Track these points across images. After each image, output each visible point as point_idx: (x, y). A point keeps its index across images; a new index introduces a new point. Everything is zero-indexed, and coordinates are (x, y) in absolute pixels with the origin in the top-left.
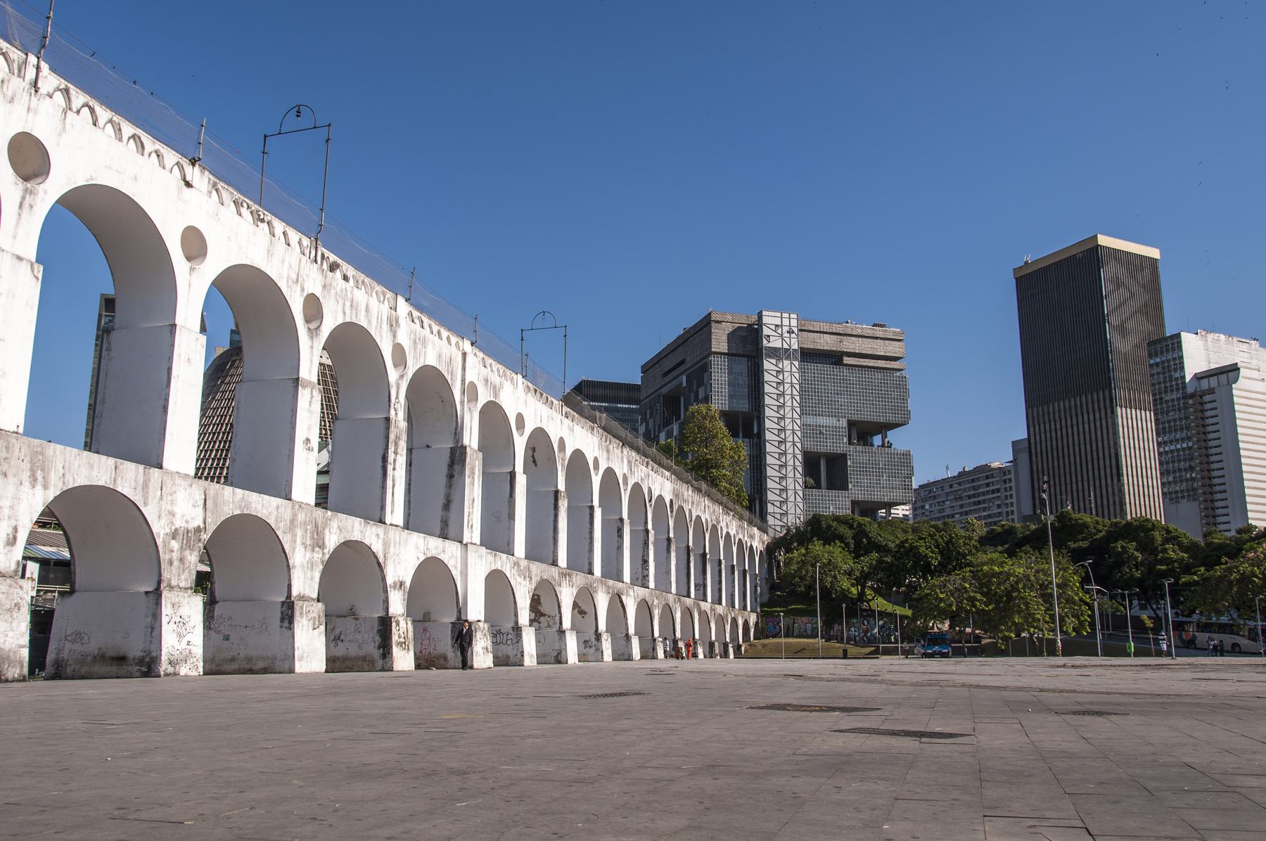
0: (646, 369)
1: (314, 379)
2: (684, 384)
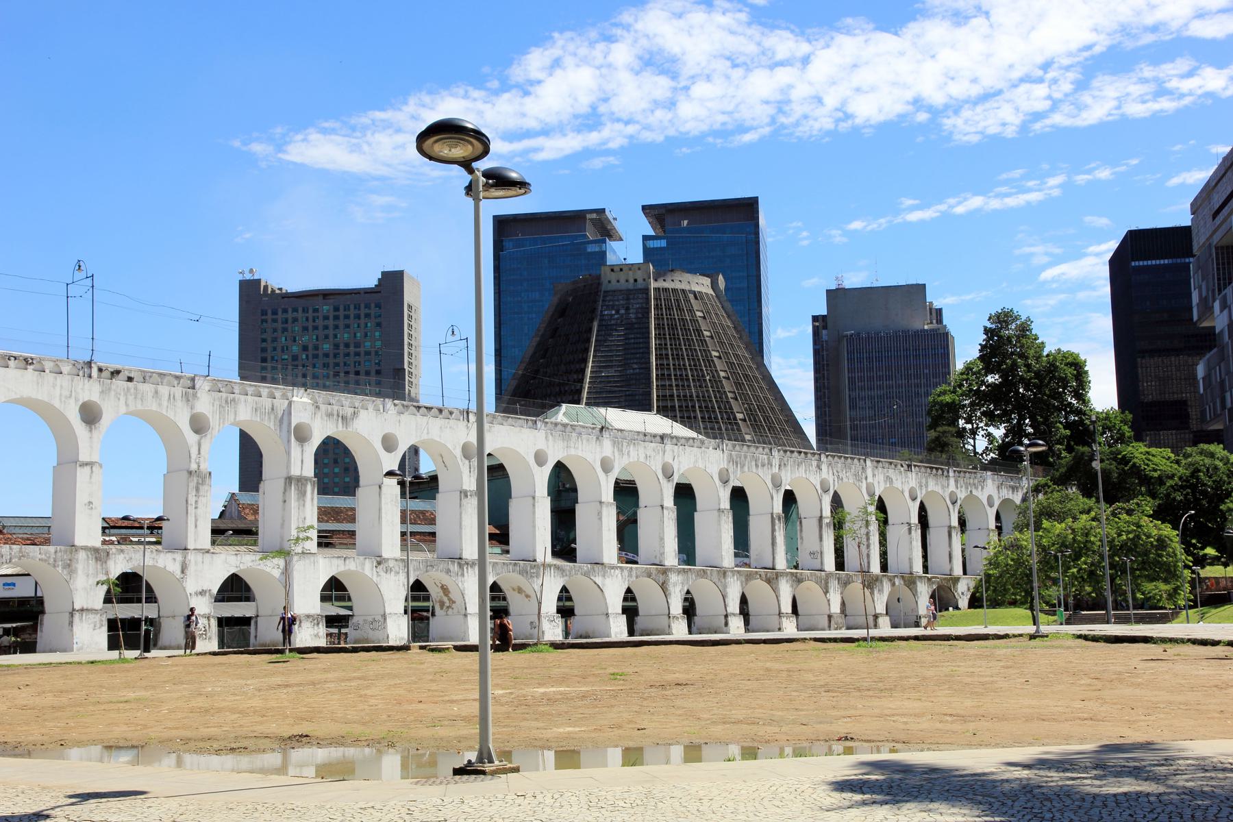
0: (1196, 208)
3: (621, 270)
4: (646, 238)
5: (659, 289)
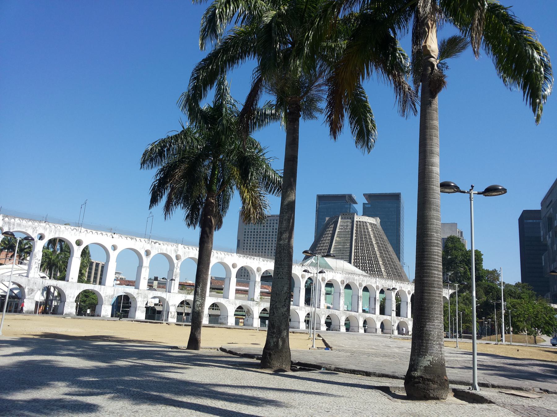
0: (542, 204)
1: (148, 265)
4: (364, 204)
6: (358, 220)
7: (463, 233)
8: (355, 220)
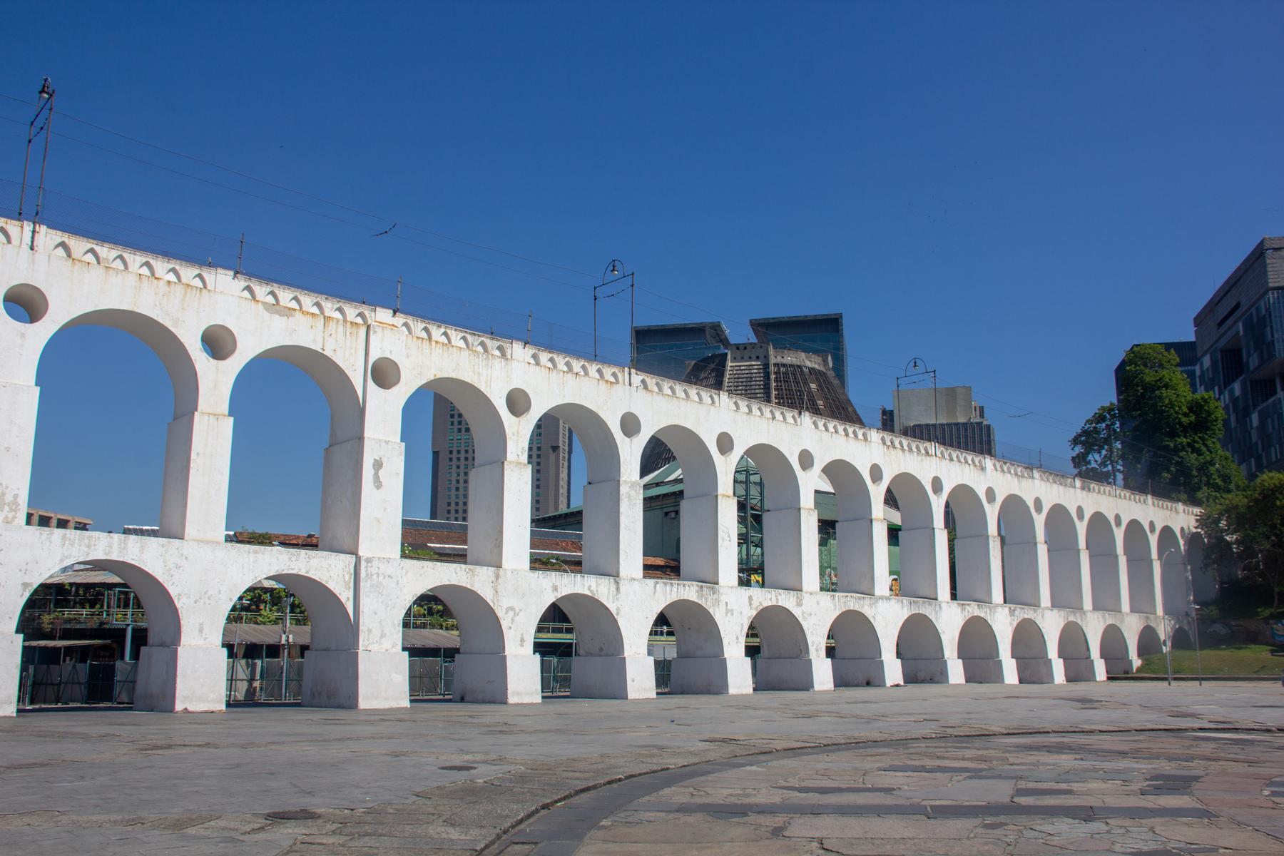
0: (1199, 321)
2: (1241, 333)
3: (745, 348)
5: (778, 364)
6: (779, 360)
7: (985, 409)
8: (773, 360)
